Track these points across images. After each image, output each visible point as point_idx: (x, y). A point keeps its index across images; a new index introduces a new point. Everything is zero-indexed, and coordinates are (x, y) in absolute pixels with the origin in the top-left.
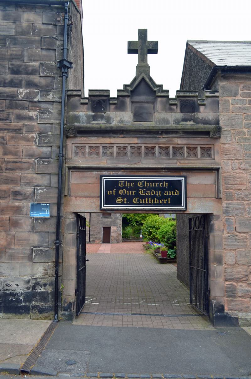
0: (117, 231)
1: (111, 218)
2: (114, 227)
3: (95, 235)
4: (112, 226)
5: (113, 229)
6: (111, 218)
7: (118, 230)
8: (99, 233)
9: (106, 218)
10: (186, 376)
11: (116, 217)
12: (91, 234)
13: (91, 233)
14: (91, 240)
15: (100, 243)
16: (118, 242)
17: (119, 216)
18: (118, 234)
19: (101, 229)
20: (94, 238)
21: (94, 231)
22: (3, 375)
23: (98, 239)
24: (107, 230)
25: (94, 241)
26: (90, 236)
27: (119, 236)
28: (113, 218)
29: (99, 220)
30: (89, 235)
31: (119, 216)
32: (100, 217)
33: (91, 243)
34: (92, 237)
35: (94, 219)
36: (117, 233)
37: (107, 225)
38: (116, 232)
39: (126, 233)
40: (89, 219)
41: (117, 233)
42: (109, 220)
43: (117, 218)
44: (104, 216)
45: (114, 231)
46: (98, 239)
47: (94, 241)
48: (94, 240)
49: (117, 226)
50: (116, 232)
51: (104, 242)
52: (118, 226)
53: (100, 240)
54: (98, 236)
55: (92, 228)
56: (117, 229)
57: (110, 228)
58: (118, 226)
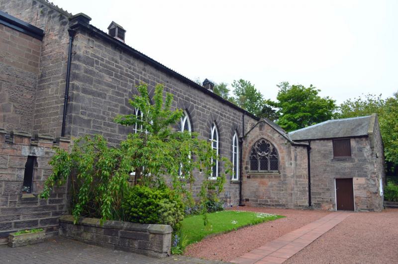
0: (368, 186)
1: (352, 161)
2: (359, 178)
3: (320, 194)
4: (354, 176)
5: (357, 182)
6: (352, 161)
7: (370, 186)
8: (328, 190)
9: (341, 160)
10: (127, 263)
11: (363, 158)
12: (311, 191)
13: (311, 189)
14: (313, 202)
15: (332, 209)
16: (371, 209)
17: (368, 156)
18: (371, 193)
19: (332, 183)
20: (319, 200)
21: (318, 185)
22: (6, 33)
23: (327, 202)
24: (345, 186)
25: (319, 205)
26: (312, 196)
27: (373, 197)
28: (356, 160)
29: (328, 165)
30: (308, 193)
31: (370, 157)
32: (329, 160)
33: (312, 209)
34: (316, 198)
35: (317, 164)
36: (369, 191)
37: (344, 174)
38: (365, 188)
39: (393, 191)
40: (307, 164)
41: (369, 191)
42: (348, 164)
43: (365, 160)
44: (336, 157)
45: (360, 187)
46: (327, 202)
47: (319, 205)
48: (319, 204)
49: (366, 176)
50: (365, 188)
51: (340, 208)
52: (369, 176)
53: (330, 203)
54: (326, 196)
55: (314, 181)
56: (367, 183)
57: (351, 179)
58: (369, 176)
